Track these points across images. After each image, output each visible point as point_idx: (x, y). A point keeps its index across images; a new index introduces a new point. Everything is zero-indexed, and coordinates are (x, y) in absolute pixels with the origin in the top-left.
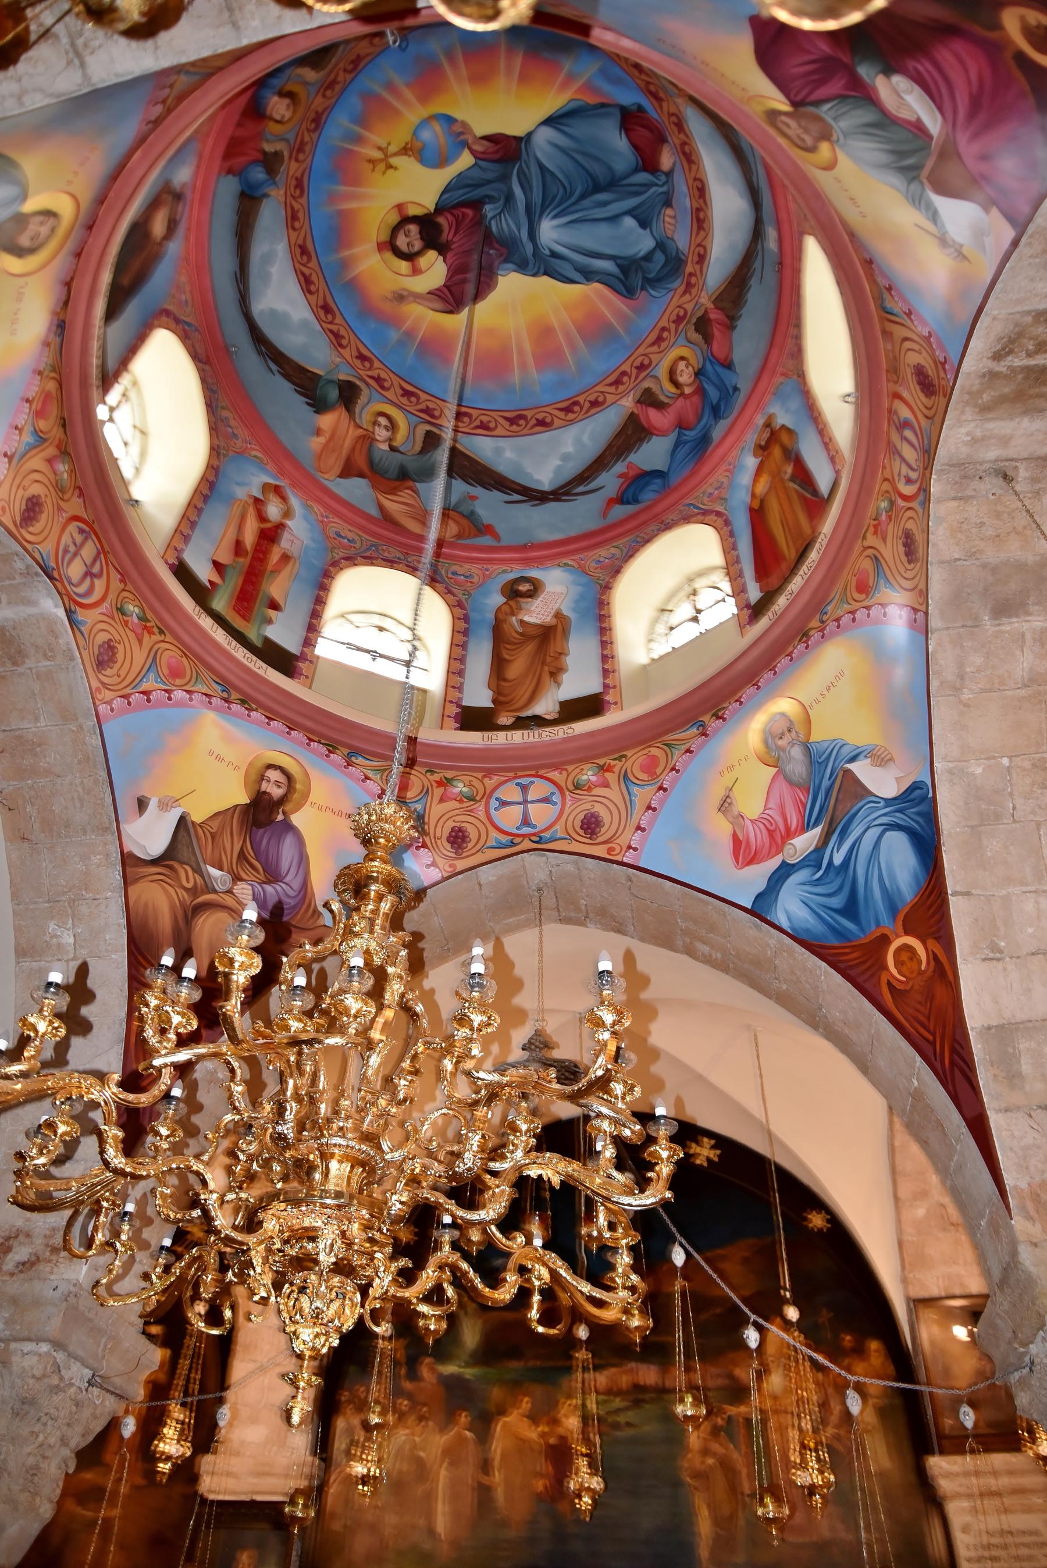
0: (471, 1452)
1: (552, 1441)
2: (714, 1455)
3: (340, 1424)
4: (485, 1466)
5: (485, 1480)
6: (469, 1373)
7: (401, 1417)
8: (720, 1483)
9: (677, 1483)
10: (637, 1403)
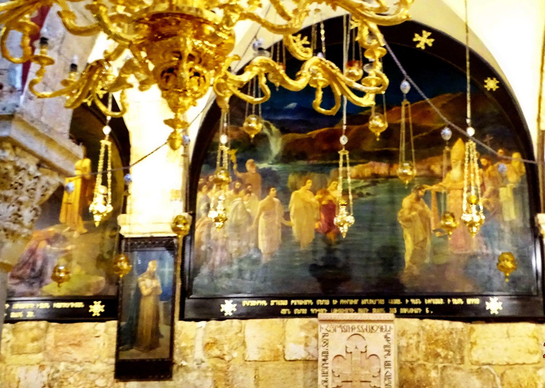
0: (278, 208)
1: (324, 202)
2: (416, 210)
3: (200, 196)
4: (287, 216)
5: (286, 223)
6: (275, 167)
7: (237, 191)
8: (419, 224)
9: (394, 224)
10: (374, 183)
